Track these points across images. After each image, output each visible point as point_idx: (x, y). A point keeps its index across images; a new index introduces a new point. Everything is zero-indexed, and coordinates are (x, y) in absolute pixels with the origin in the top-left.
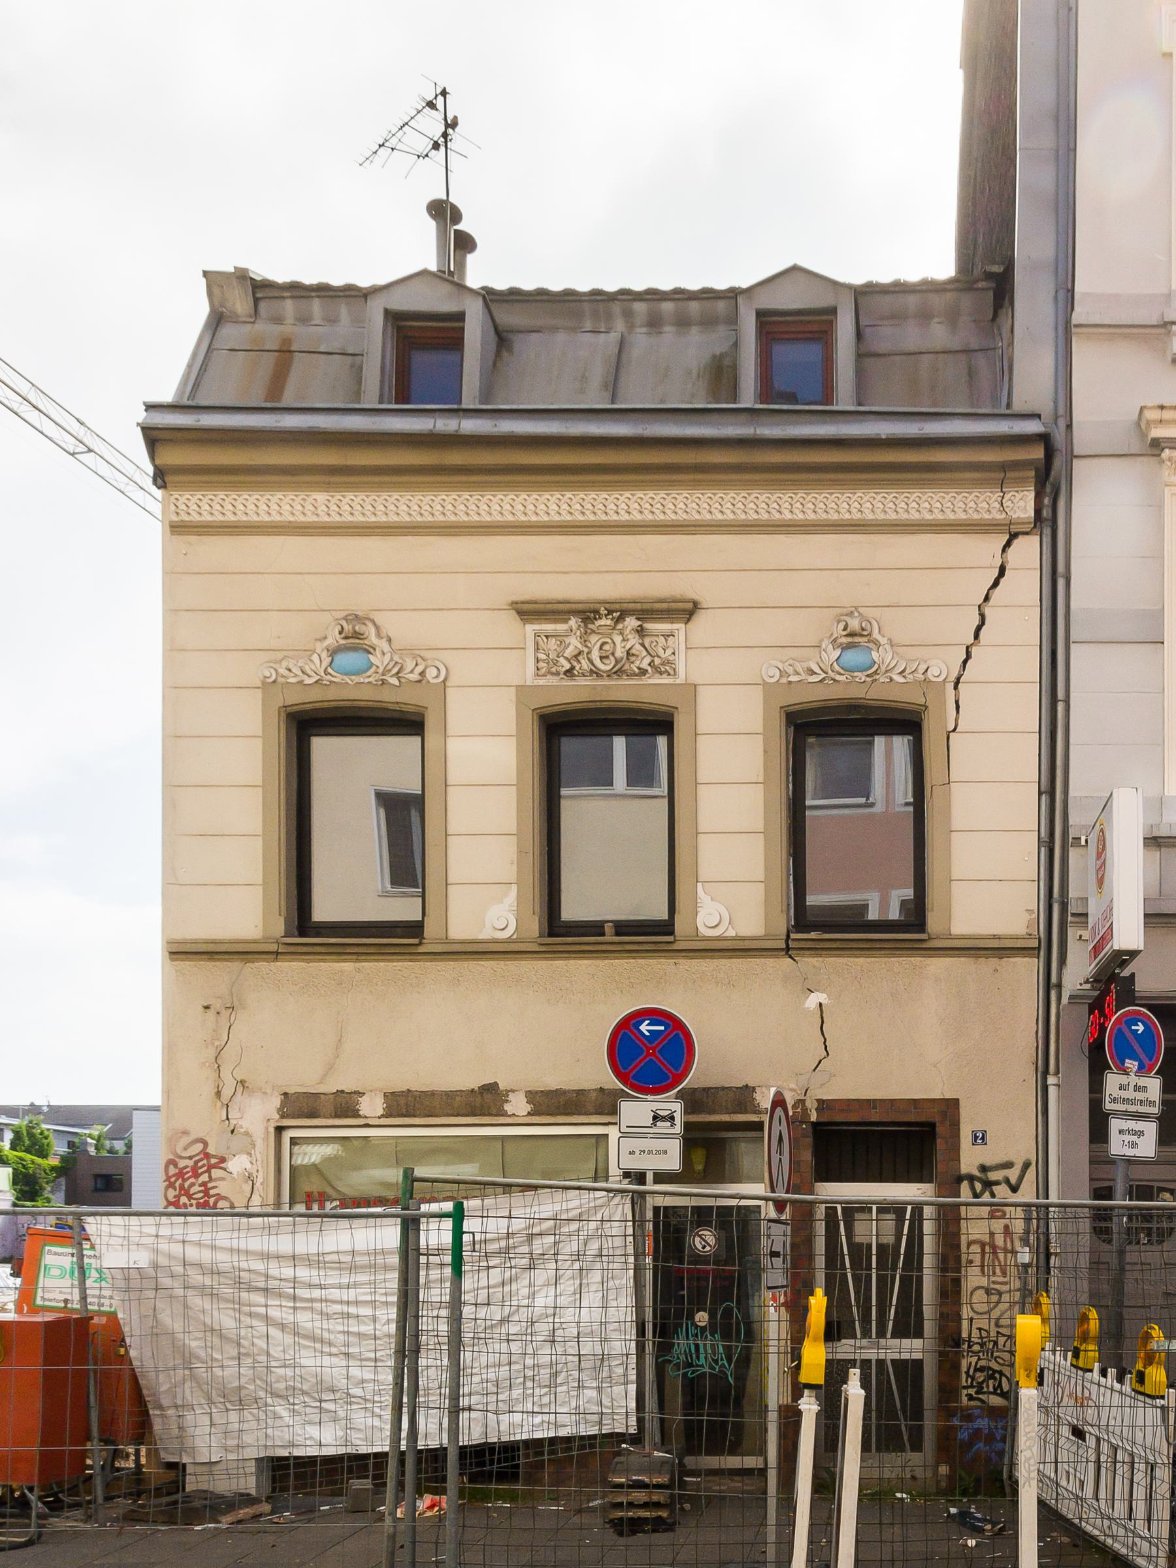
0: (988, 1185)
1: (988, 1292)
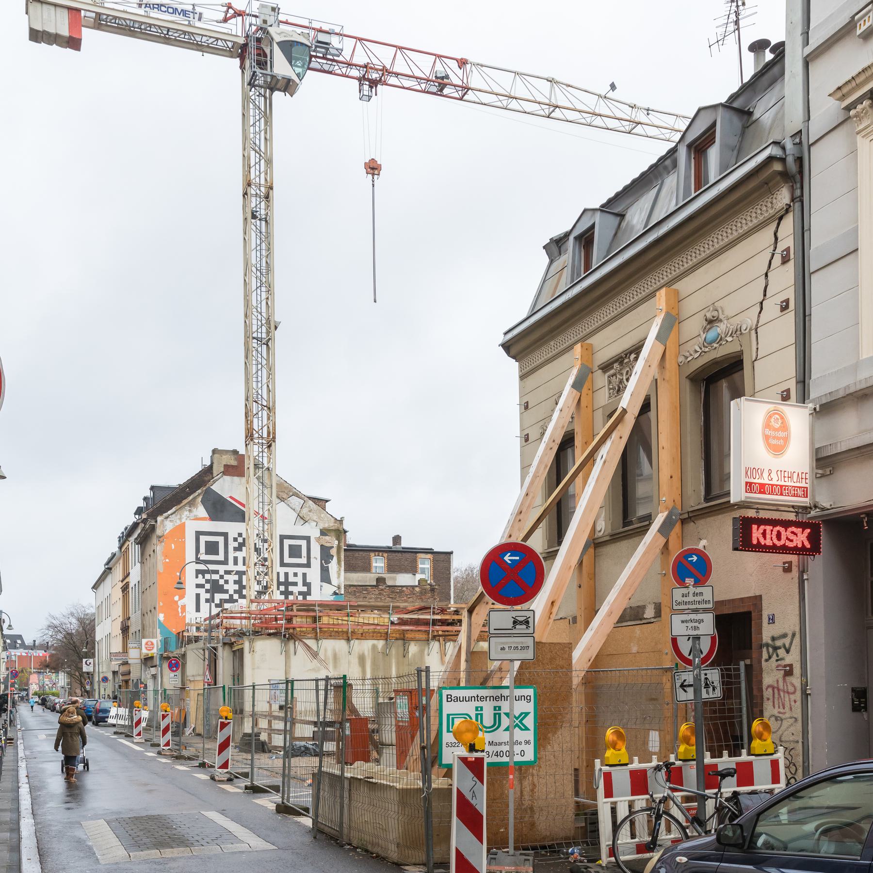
0: (776, 649)
1: (776, 719)
